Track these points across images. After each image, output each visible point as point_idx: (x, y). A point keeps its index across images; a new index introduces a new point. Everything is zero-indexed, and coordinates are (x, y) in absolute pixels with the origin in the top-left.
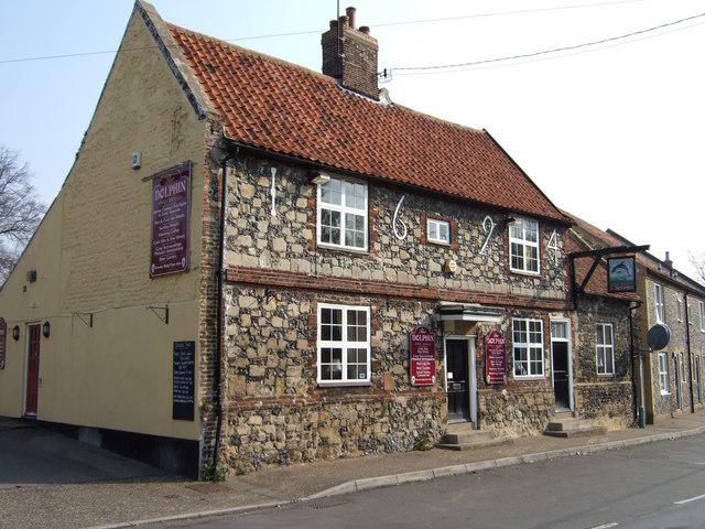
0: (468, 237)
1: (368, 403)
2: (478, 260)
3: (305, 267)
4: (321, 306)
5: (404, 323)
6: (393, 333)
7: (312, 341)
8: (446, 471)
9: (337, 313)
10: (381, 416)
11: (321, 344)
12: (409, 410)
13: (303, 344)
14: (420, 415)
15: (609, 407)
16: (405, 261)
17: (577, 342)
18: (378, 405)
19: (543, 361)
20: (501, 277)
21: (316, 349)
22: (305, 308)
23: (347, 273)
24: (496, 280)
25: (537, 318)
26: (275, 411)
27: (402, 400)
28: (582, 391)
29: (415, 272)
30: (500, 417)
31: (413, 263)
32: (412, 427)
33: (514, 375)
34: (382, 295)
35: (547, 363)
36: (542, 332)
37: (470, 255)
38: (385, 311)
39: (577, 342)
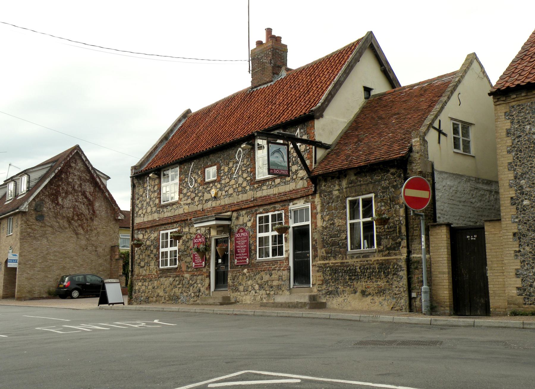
0: (226, 169)
1: (173, 277)
2: (233, 182)
3: (156, 216)
4: (258, 216)
5: (192, 234)
6: (187, 240)
7: (158, 249)
8: (506, 323)
9: (267, 218)
10: (179, 284)
11: (161, 250)
12: (191, 282)
13: (155, 251)
14: (195, 285)
15: (360, 285)
16: (193, 199)
17: (320, 223)
18: (177, 279)
19: (284, 245)
20: (248, 188)
21: (159, 253)
22: (156, 235)
23: (169, 214)
24: (244, 191)
25: (278, 210)
26: (145, 280)
27: (187, 275)
28: (322, 269)
29: (197, 203)
30: (241, 288)
31: (197, 199)
32: (191, 291)
33: (258, 258)
34: (182, 221)
35: (288, 246)
36: (258, 225)
37: (227, 180)
38: (184, 229)
39: (320, 223)
